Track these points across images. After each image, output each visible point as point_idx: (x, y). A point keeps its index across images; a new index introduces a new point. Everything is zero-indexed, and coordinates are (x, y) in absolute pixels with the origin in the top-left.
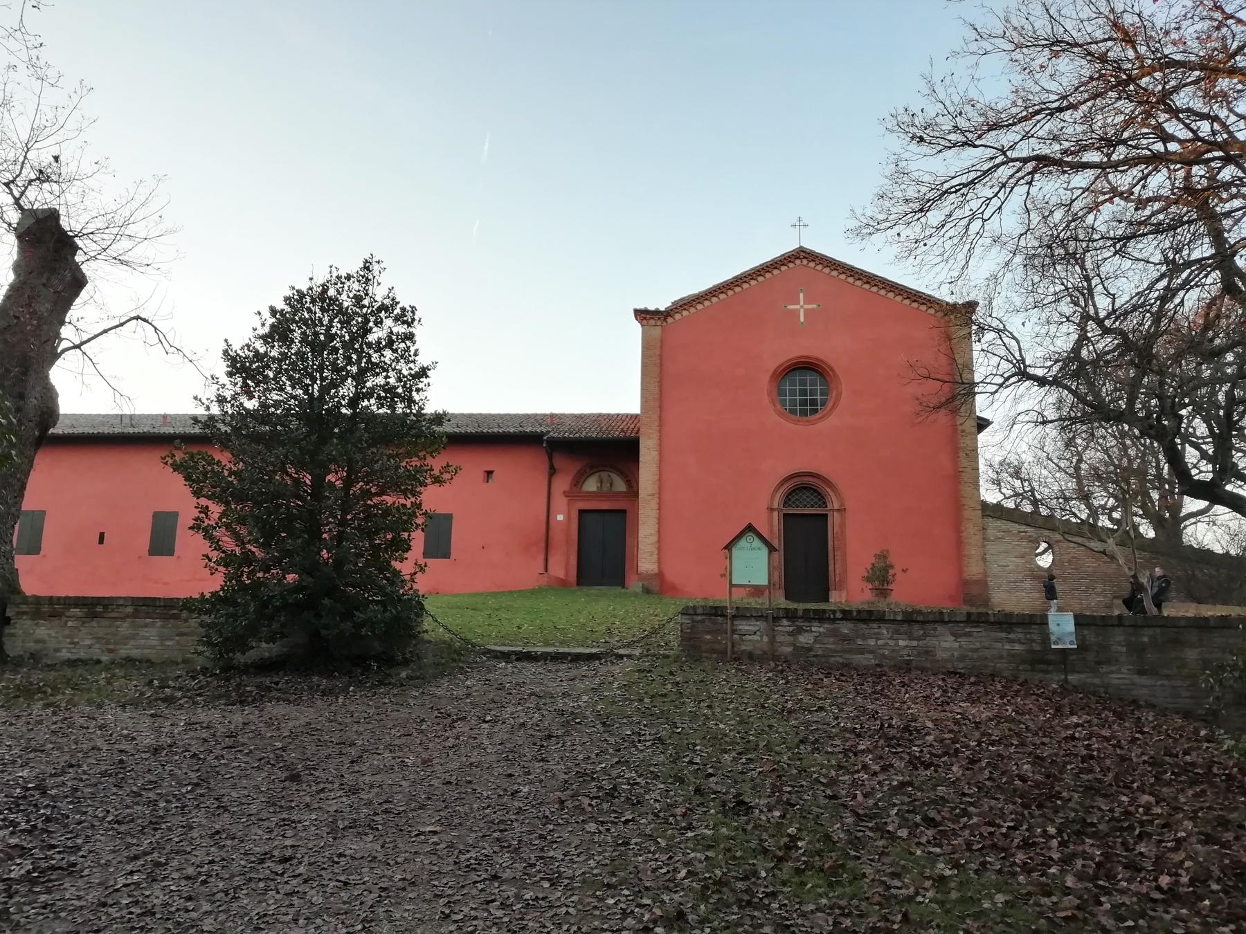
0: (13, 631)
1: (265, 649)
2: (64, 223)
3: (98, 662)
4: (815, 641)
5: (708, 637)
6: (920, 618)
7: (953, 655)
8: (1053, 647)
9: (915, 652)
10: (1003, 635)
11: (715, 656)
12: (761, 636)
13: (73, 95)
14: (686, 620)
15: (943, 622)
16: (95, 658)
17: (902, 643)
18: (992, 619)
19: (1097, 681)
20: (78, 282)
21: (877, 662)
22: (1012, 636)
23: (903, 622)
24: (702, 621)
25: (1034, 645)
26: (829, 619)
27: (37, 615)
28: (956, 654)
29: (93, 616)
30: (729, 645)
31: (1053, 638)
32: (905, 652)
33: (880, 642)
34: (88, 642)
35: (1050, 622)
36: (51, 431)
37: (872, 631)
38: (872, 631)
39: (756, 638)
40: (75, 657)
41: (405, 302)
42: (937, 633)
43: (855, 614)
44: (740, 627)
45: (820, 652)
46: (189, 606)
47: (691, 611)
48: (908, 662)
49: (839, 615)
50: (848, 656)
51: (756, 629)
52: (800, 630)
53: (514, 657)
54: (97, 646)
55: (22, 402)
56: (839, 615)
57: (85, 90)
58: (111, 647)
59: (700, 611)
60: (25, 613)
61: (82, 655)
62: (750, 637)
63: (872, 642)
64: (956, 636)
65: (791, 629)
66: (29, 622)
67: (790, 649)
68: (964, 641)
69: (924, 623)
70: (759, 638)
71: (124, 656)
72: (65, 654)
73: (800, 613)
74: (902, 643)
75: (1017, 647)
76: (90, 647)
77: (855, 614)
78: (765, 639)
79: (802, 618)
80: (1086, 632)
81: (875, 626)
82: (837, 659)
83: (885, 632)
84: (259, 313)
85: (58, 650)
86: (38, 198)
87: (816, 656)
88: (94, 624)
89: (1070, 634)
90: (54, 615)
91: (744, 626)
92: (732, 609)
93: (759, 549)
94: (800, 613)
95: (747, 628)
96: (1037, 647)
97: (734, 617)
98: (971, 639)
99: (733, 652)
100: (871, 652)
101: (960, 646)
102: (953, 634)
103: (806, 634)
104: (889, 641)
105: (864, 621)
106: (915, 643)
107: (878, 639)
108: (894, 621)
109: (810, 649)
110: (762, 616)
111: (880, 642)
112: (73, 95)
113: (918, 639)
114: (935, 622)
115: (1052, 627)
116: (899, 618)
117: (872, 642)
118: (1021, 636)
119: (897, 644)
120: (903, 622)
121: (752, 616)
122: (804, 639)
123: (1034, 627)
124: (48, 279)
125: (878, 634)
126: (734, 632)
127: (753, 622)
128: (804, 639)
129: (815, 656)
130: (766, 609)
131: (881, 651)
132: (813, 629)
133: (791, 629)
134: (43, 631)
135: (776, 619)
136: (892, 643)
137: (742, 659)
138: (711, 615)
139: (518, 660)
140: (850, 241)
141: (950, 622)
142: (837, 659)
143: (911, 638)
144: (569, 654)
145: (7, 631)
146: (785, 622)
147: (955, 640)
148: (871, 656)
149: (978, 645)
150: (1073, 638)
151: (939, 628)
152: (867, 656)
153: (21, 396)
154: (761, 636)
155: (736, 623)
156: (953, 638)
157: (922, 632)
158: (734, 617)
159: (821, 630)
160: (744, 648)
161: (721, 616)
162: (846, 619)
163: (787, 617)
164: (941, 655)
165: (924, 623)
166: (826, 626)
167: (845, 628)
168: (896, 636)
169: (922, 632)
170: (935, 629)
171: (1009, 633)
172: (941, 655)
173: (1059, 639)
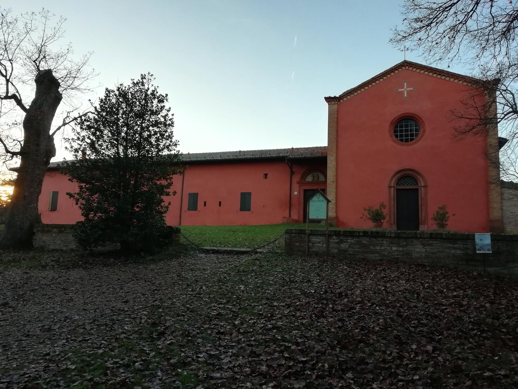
0: (36, 238)
1: (109, 247)
2: (54, 74)
3: (62, 250)
4: (349, 247)
5: (297, 244)
6: (404, 236)
7: (422, 255)
8: (477, 252)
9: (401, 254)
10: (451, 245)
11: (300, 253)
12: (323, 244)
13: (59, 23)
14: (287, 236)
15: (417, 238)
16: (61, 249)
17: (394, 249)
18: (444, 236)
19: (506, 272)
20: (58, 98)
21: (381, 258)
22: (456, 246)
23: (395, 237)
24: (294, 236)
25: (469, 251)
26: (356, 236)
27: (43, 231)
28: (423, 255)
29: (61, 232)
30: (307, 248)
31: (477, 247)
32: (396, 253)
33: (382, 248)
34: (59, 242)
35: (476, 238)
36: (53, 160)
37: (379, 242)
38: (379, 242)
39: (320, 245)
40: (55, 248)
41: (161, 92)
42: (413, 243)
43: (369, 233)
44: (313, 240)
45: (351, 253)
46: (72, 227)
47: (289, 232)
48: (397, 259)
49: (361, 234)
50: (366, 255)
51: (320, 240)
52: (341, 241)
53: (211, 252)
54: (62, 244)
55: (38, 148)
56: (361, 234)
57: (63, 20)
58: (67, 244)
59: (294, 232)
60: (39, 231)
61: (57, 247)
62: (317, 245)
63: (378, 248)
64: (424, 245)
65: (337, 240)
66: (41, 234)
67: (336, 251)
68: (428, 248)
69: (406, 238)
70: (321, 245)
71: (71, 248)
72: (52, 247)
73: (342, 233)
74: (394, 249)
75: (458, 252)
76: (60, 244)
77: (369, 233)
78: (325, 245)
79: (342, 235)
80: (500, 244)
81: (380, 239)
82: (360, 256)
83: (385, 243)
84: (90, 100)
85: (49, 245)
86: (44, 66)
87: (349, 254)
88: (61, 235)
89: (488, 245)
90: (49, 231)
91: (314, 239)
92: (308, 230)
93: (322, 201)
94: (342, 233)
95: (316, 240)
96: (470, 252)
97: (310, 235)
98: (432, 247)
99: (309, 252)
100: (377, 253)
101: (426, 251)
102: (422, 244)
103: (345, 243)
104: (387, 248)
105: (375, 237)
106: (401, 249)
107: (381, 246)
108: (390, 237)
109: (346, 251)
110: (323, 234)
111: (382, 248)
112: (59, 23)
113: (403, 247)
114: (412, 238)
115: (477, 241)
116: (393, 235)
117: (378, 248)
118: (461, 246)
119: (391, 249)
120: (395, 237)
121: (318, 234)
122: (344, 246)
123: (469, 241)
124: (46, 98)
125: (382, 243)
126: (309, 241)
127: (319, 237)
128: (344, 246)
129: (348, 254)
130: (325, 231)
131: (383, 253)
132: (348, 241)
133: (337, 240)
134: (45, 238)
135: (330, 236)
136: (389, 248)
137: (309, 254)
138: (299, 233)
139: (213, 253)
140: (394, 46)
141: (420, 238)
142: (360, 256)
143: (400, 246)
144: (235, 251)
145: (34, 238)
146: (334, 237)
147: (423, 248)
148: (377, 255)
149: (436, 250)
150: (490, 247)
151: (415, 241)
152: (375, 255)
153: (38, 145)
154: (323, 244)
155: (310, 237)
156: (422, 247)
157: (405, 243)
158: (310, 235)
159: (352, 241)
160: (314, 250)
161: (303, 234)
162: (365, 236)
163: (335, 235)
164: (415, 255)
165: (406, 238)
166: (355, 239)
167: (365, 241)
168: (391, 245)
169: (405, 243)
170: (412, 242)
171: (454, 244)
172: (415, 255)
173: (481, 247)
